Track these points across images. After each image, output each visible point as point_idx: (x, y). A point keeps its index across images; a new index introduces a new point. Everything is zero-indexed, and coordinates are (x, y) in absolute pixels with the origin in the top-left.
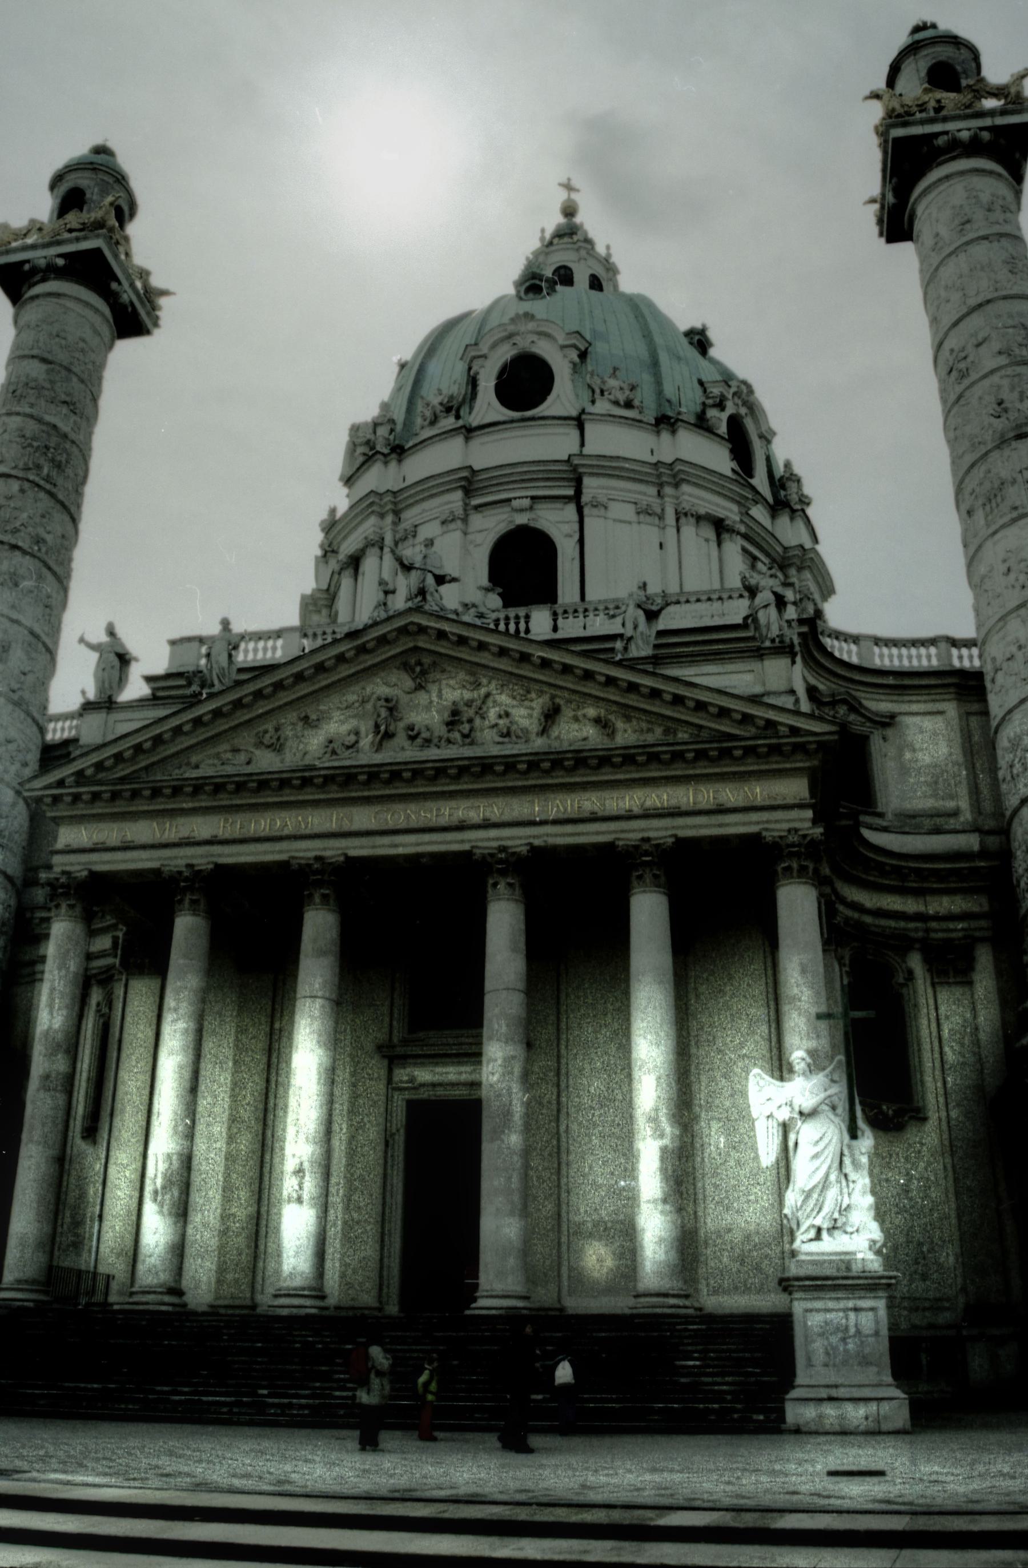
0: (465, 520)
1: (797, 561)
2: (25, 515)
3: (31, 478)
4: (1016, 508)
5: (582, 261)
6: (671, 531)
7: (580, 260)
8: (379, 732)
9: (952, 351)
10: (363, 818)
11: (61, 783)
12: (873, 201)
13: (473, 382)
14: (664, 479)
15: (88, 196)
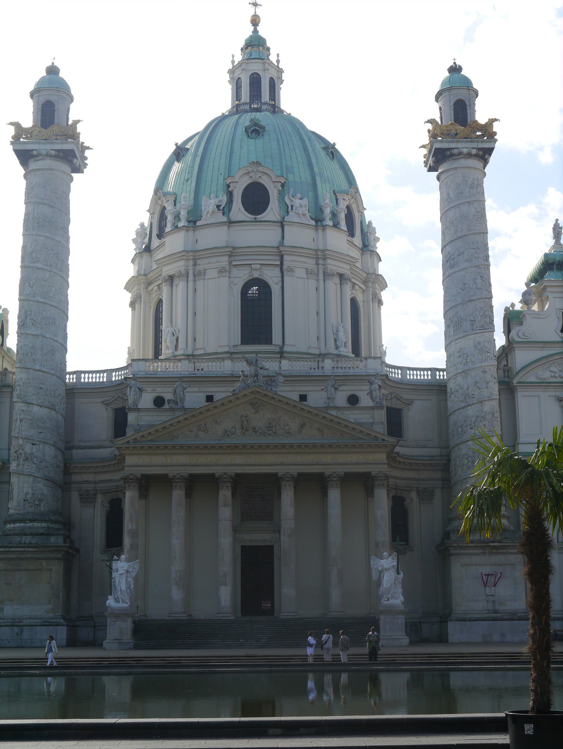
0: (229, 272)
1: (372, 280)
2: (54, 289)
3: (54, 270)
4: (465, 332)
5: (266, 71)
6: (321, 282)
7: (265, 70)
8: (244, 429)
9: (449, 253)
10: (239, 459)
11: (128, 442)
12: (423, 146)
13: (230, 195)
14: (319, 257)
15: (56, 107)
